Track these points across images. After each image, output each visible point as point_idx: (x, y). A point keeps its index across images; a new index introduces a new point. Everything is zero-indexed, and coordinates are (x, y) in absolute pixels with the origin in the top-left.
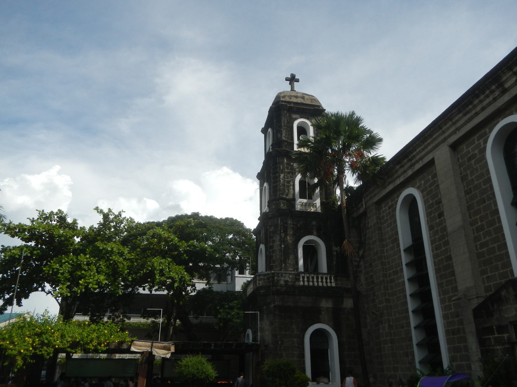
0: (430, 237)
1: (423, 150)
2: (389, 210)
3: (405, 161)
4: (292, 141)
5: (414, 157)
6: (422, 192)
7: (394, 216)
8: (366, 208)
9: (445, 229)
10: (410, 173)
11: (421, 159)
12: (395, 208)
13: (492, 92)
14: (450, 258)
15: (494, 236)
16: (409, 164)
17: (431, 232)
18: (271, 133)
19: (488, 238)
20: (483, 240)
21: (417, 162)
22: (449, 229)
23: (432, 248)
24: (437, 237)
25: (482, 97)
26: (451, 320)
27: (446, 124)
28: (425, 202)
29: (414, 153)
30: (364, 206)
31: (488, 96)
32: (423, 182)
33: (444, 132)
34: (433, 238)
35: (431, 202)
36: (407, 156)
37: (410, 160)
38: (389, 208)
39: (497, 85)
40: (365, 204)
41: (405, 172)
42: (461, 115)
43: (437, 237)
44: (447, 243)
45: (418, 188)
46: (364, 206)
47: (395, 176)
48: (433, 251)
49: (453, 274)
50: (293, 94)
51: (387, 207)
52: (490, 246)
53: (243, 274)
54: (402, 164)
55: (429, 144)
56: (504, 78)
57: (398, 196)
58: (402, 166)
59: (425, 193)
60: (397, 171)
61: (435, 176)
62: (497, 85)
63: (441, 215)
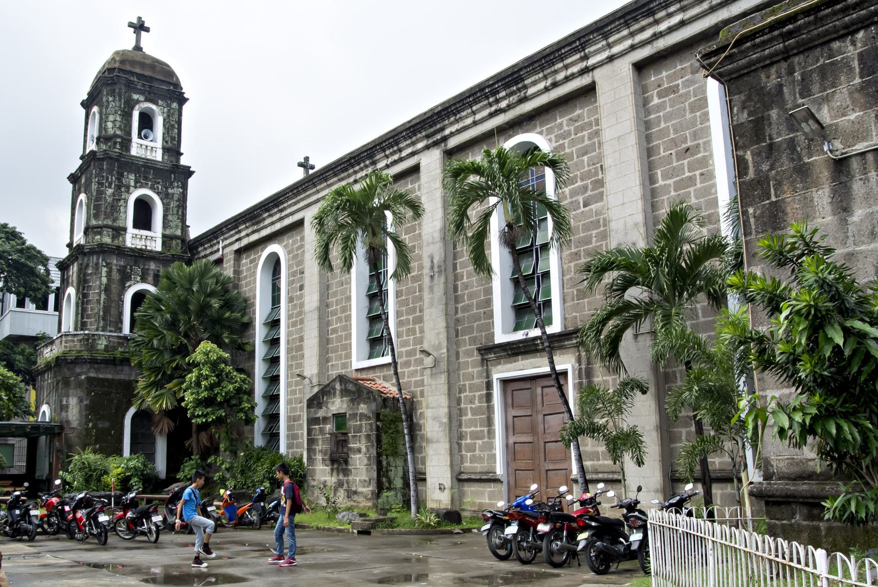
0: (288, 311)
1: (295, 204)
2: (250, 264)
3: (276, 210)
4: (127, 137)
5: (285, 209)
6: (289, 253)
7: (255, 273)
8: (222, 255)
9: (302, 305)
10: (278, 226)
11: (292, 214)
12: (257, 264)
13: (366, 166)
14: (301, 339)
15: (344, 323)
16: (278, 216)
17: (290, 305)
18: (97, 116)
19: (339, 325)
20: (335, 326)
21: (287, 216)
22: (307, 308)
23: (289, 323)
24: (295, 312)
25: (357, 168)
26: (294, 406)
27: (320, 183)
28: (289, 267)
29: (285, 205)
30: (221, 252)
31: (362, 169)
32: (291, 241)
33: (318, 192)
34: (290, 312)
35: (295, 269)
36: (277, 206)
37: (281, 211)
38: (251, 262)
39: (371, 161)
40: (223, 249)
41: (272, 223)
42: (335, 179)
43: (295, 312)
44: (302, 322)
45: (285, 247)
46: (221, 252)
47: (262, 225)
48: (288, 327)
49: (303, 356)
50: (138, 59)
51: (248, 260)
52: (339, 334)
53: (24, 307)
54: (271, 212)
55: (302, 199)
56: (378, 157)
57: (262, 250)
58: (271, 216)
59: (291, 255)
60: (264, 219)
61: (302, 239)
62: (371, 161)
63: (301, 288)
